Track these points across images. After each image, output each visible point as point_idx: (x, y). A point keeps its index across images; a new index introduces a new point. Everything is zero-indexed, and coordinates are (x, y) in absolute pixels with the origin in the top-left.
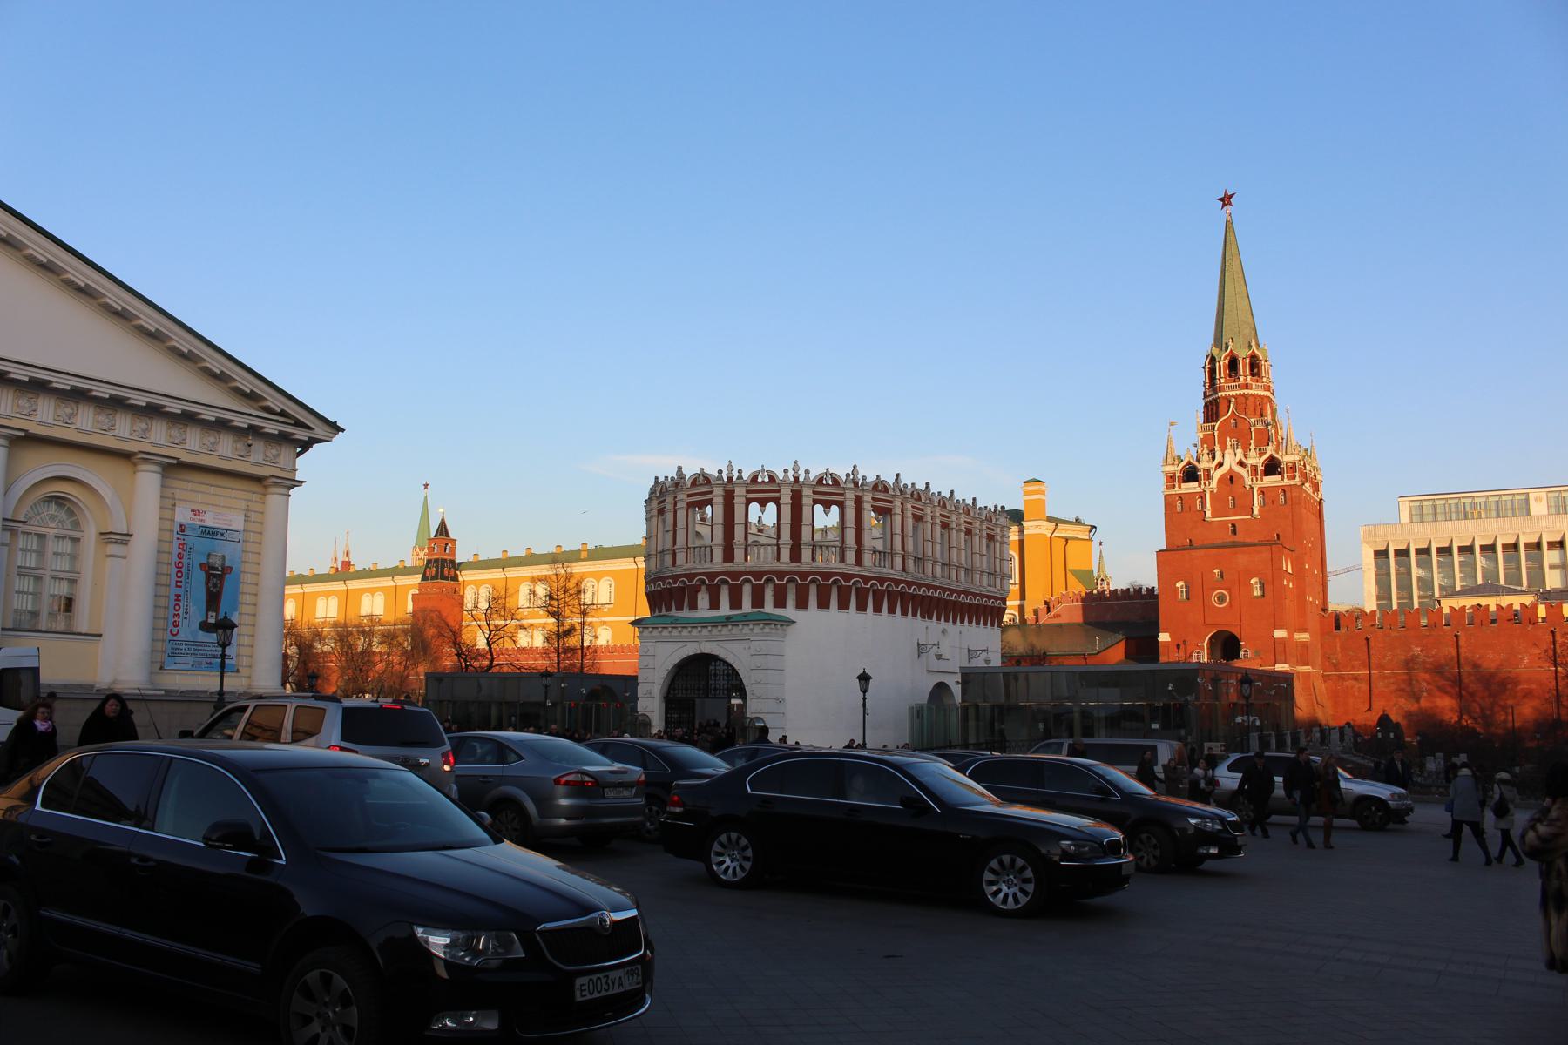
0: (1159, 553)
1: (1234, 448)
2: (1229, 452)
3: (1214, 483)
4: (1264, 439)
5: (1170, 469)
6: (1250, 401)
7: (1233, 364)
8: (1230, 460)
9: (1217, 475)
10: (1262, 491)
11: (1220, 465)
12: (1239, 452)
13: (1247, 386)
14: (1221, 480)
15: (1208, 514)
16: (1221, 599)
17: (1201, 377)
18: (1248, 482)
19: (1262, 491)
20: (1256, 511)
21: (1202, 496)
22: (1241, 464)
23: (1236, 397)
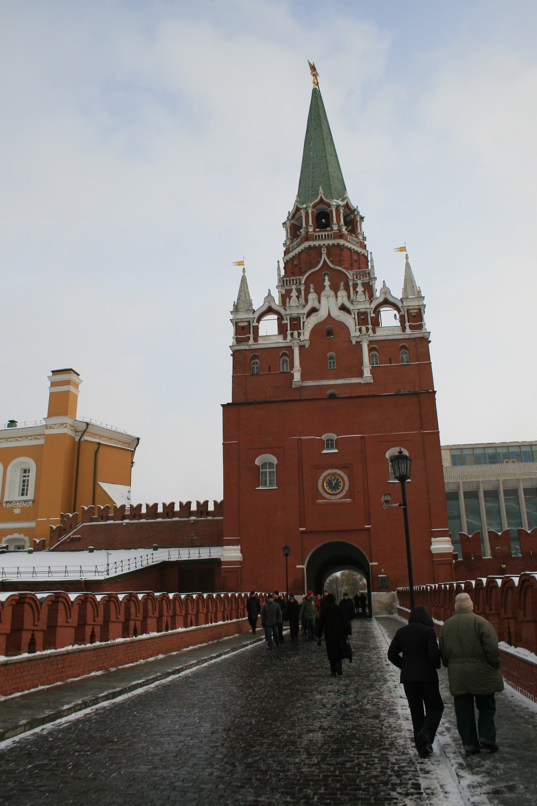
0: (226, 407)
1: (335, 289)
2: (328, 291)
3: (306, 335)
4: (369, 289)
5: (242, 316)
6: (346, 254)
7: (323, 219)
10: (374, 346)
11: (314, 310)
12: (342, 293)
14: (314, 331)
15: (297, 377)
17: (282, 235)
18: (354, 332)
19: (374, 346)
20: (367, 373)
22: (343, 308)
23: (328, 247)
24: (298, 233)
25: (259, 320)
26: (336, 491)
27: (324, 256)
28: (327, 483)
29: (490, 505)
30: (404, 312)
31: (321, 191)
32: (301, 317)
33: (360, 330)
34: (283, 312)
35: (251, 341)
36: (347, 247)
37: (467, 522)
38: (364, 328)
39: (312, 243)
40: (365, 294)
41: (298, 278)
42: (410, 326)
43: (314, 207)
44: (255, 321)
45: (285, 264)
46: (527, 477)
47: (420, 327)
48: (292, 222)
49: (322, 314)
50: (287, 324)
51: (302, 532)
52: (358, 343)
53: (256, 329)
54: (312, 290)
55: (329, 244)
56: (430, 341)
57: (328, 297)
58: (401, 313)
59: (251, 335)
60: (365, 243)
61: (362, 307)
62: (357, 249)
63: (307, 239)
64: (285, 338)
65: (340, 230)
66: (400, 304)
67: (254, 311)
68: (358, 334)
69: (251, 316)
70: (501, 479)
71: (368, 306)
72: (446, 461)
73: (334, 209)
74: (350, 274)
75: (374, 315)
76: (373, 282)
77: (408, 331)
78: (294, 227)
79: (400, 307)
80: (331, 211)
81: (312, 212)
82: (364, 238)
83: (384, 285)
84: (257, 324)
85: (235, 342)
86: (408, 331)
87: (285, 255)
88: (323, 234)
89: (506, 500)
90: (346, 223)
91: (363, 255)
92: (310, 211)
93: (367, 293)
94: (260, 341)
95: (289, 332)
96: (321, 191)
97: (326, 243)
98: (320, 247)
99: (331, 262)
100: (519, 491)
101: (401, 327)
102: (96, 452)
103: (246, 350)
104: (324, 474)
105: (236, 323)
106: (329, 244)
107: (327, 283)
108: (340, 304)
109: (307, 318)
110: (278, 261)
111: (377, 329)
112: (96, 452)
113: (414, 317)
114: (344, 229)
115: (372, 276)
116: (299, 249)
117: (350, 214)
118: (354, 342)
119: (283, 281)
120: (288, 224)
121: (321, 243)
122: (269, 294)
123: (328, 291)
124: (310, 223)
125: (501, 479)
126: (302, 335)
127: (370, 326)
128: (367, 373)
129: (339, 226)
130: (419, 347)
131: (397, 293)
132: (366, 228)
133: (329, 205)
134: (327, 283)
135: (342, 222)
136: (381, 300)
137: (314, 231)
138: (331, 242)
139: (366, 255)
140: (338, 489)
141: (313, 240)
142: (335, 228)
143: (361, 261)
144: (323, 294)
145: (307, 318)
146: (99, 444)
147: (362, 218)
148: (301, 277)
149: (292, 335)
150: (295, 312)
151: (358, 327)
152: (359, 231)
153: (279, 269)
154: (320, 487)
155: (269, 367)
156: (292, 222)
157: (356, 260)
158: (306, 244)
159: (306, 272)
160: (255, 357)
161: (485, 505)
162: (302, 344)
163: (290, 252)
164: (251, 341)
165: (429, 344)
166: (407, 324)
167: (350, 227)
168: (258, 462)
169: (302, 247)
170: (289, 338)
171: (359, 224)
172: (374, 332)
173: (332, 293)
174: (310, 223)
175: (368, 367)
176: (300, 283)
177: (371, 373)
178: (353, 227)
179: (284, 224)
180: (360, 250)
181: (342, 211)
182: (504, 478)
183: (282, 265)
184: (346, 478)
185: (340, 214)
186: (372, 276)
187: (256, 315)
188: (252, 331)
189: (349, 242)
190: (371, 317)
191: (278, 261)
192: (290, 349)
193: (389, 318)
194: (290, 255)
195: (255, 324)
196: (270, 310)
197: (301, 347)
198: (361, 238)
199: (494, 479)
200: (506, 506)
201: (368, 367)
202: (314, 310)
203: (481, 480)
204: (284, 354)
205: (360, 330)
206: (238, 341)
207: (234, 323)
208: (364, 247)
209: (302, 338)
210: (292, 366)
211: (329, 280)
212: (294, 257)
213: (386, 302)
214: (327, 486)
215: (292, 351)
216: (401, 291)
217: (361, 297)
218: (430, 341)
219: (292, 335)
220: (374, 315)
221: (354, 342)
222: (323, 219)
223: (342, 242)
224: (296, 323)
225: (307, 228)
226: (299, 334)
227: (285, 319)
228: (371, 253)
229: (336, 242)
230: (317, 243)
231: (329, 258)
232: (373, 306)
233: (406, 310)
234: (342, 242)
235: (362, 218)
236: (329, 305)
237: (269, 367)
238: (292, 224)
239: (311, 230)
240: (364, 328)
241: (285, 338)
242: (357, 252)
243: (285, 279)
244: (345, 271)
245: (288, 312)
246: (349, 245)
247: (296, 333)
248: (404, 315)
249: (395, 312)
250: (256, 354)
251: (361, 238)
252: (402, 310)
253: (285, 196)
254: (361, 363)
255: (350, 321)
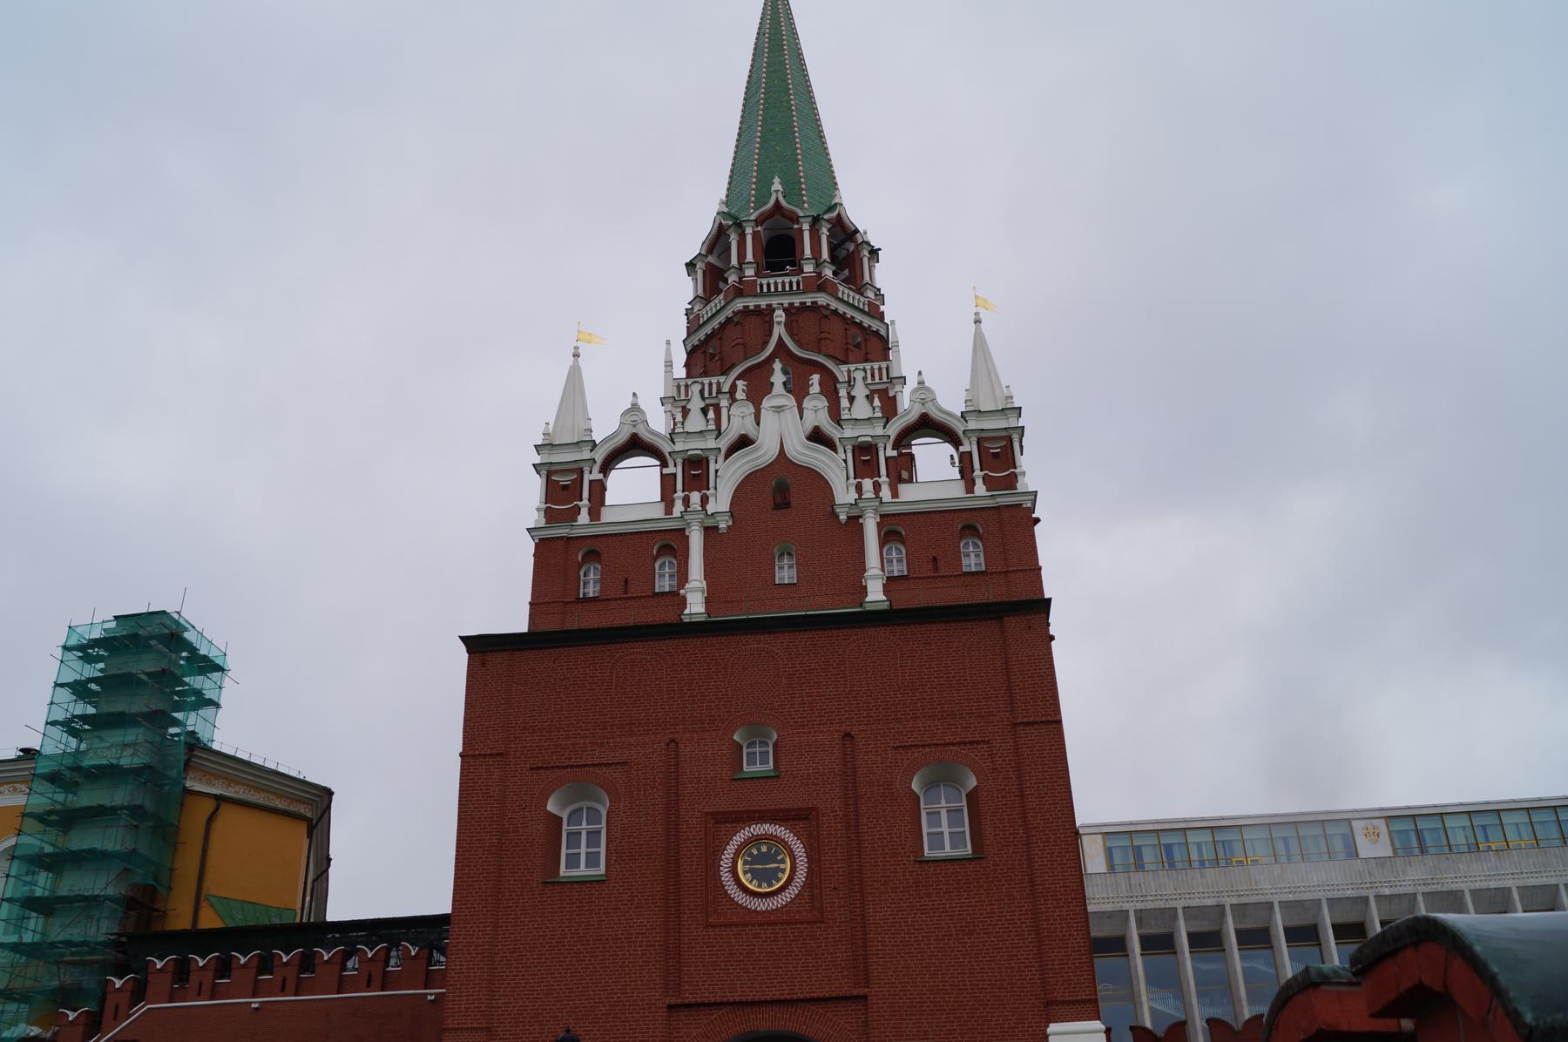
1: (798, 390)
2: (779, 396)
3: (721, 502)
7: (779, 250)
8: (781, 426)
9: (727, 476)
10: (894, 528)
11: (743, 442)
13: (822, 286)
16: (763, 860)
17: (686, 289)
18: (844, 494)
19: (894, 528)
20: (875, 594)
21: (672, 543)
22: (817, 436)
24: (721, 285)
25: (608, 465)
26: (770, 885)
27: (779, 331)
28: (745, 863)
29: (1204, 967)
30: (969, 446)
31: (777, 185)
32: (712, 459)
33: (859, 488)
34: (666, 448)
35: (583, 518)
36: (836, 311)
37: (1151, 1009)
38: (867, 484)
39: (752, 303)
40: (871, 403)
41: (714, 380)
42: (985, 479)
43: (758, 222)
44: (596, 468)
45: (690, 354)
46: (1291, 897)
47: (1011, 482)
48: (710, 259)
49: (764, 452)
50: (675, 475)
51: (670, 1007)
52: (855, 522)
53: (599, 489)
54: (740, 395)
55: (791, 304)
56: (1037, 520)
57: (779, 409)
58: (962, 449)
59: (585, 501)
60: (882, 308)
61: (865, 433)
62: (859, 317)
63: (739, 293)
64: (669, 510)
65: (819, 275)
66: (959, 427)
67: (594, 445)
68: (852, 496)
69: (586, 455)
70: (1228, 901)
71: (879, 431)
72: (1094, 859)
73: (806, 227)
74: (841, 372)
75: (895, 453)
76: (898, 388)
77: (980, 489)
78: (711, 269)
79: (961, 434)
80: (801, 231)
81: (755, 234)
82: (880, 296)
83: (921, 383)
84: (600, 476)
85: (542, 523)
86: (980, 489)
87: (689, 335)
88: (779, 280)
89: (1242, 958)
90: (834, 258)
91: (877, 333)
92: (749, 231)
93: (877, 402)
94: (607, 516)
95: (680, 494)
96: (777, 185)
97: (786, 301)
98: (771, 310)
99: (799, 343)
100: (1273, 932)
101: (962, 483)
102: (211, 819)
103: (568, 539)
104: (739, 838)
105: (548, 471)
106: (791, 304)
107: (778, 378)
108: (809, 427)
109: (726, 458)
110: (668, 342)
111: (902, 488)
112: (211, 819)
113: (995, 453)
114: (828, 272)
115: (894, 374)
116: (721, 318)
117: (843, 242)
118: (843, 517)
119: (679, 387)
120: (700, 266)
121: (774, 302)
122: (635, 408)
123: (779, 396)
124: (749, 257)
125: (1228, 901)
126: (711, 500)
127: (884, 479)
128: (875, 594)
129: (818, 265)
130: (1010, 526)
131: (951, 401)
132: (883, 275)
133: (795, 219)
134: (778, 378)
135: (825, 255)
136: (913, 417)
137: (757, 274)
138: (797, 301)
139: (883, 332)
140: (778, 880)
141: (756, 296)
142: (809, 268)
143: (871, 342)
144: (767, 403)
145: (726, 458)
146: (216, 797)
147: (874, 253)
148: (722, 379)
149: (686, 501)
150: (695, 446)
151: (852, 480)
152: (867, 278)
153: (669, 364)
154: (726, 877)
155: (626, 581)
156: (710, 259)
157: (858, 346)
158: (739, 304)
159: (733, 366)
160: (593, 556)
161: (1194, 968)
162: (710, 522)
163: (701, 326)
164: (583, 518)
165: (1037, 528)
166: (978, 473)
167: (846, 272)
168: (551, 807)
169: (728, 313)
170: (678, 508)
171: (865, 260)
172: (895, 494)
173: (790, 401)
174: (749, 257)
175: (875, 577)
176: (719, 392)
177: (886, 592)
178: (852, 272)
179: (690, 266)
180: (867, 322)
181: (824, 232)
182: (1235, 901)
183: (680, 357)
184: (799, 849)
185: (819, 238)
186: (894, 374)
187: (599, 456)
188: (586, 494)
189: (842, 300)
190: (887, 459)
191: (668, 342)
192: (681, 535)
193: (935, 463)
194: (701, 335)
195: (597, 476)
196: (635, 445)
197: (710, 532)
198: (870, 294)
199: (1209, 902)
200: (1244, 969)
201: (875, 577)
202: (743, 442)
203: (1179, 904)
204: (666, 550)
205: (859, 488)
206: (551, 516)
207: (544, 473)
208: (881, 317)
209: (711, 508)
210: (683, 576)
211: (785, 372)
212: (709, 337)
213: (928, 425)
214: (745, 873)
215: (685, 541)
216: (963, 396)
217: (862, 409)
218: (1037, 520)
219: (686, 501)
220: (895, 453)
221: (843, 517)
222: (779, 250)
223: (822, 299)
224: (697, 471)
225: (741, 269)
226: (704, 500)
227: (671, 463)
228: (893, 322)
229: (808, 299)
230: (763, 303)
231: (792, 334)
232: (894, 428)
233: (974, 440)
234: (822, 299)
235: (874, 253)
236: (781, 426)
237: (626, 581)
238: (709, 265)
239: (750, 272)
240: (867, 484)
241: (669, 510)
242: (860, 325)
243: (682, 383)
244: (829, 364)
245: (679, 447)
246: (842, 309)
247: (695, 497)
248: (970, 453)
249: (948, 449)
250: (596, 548)
251: (870, 294)
252: (965, 441)
253: (696, 200)
254: (862, 568)
255: (835, 469)
